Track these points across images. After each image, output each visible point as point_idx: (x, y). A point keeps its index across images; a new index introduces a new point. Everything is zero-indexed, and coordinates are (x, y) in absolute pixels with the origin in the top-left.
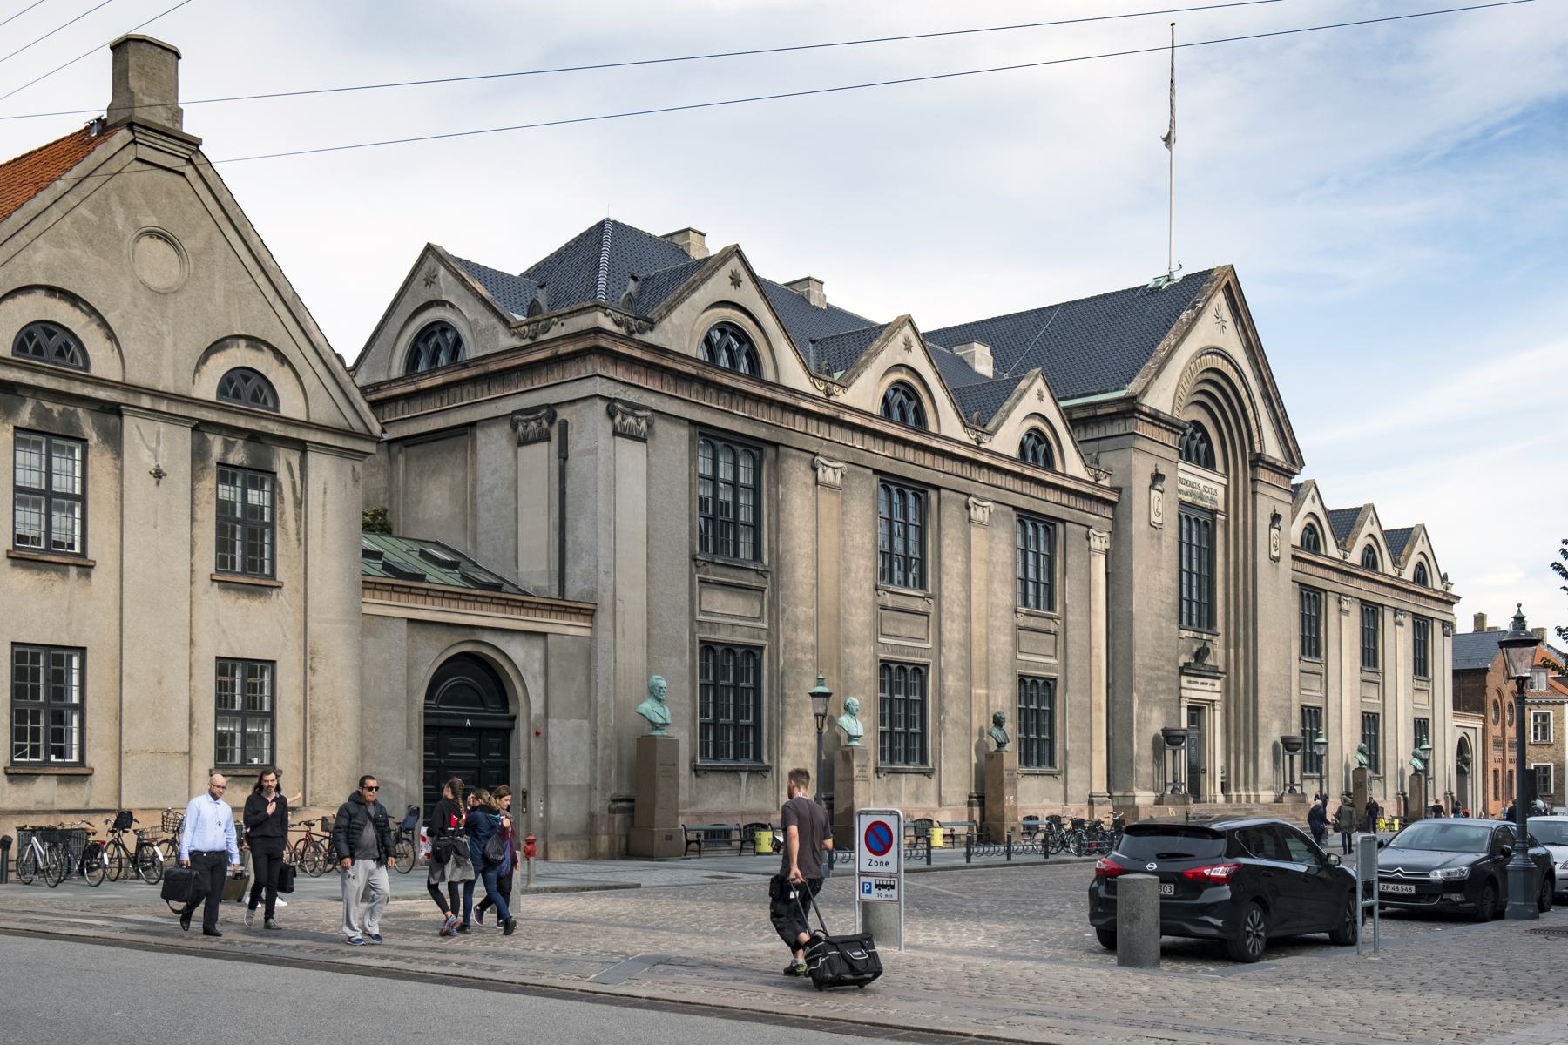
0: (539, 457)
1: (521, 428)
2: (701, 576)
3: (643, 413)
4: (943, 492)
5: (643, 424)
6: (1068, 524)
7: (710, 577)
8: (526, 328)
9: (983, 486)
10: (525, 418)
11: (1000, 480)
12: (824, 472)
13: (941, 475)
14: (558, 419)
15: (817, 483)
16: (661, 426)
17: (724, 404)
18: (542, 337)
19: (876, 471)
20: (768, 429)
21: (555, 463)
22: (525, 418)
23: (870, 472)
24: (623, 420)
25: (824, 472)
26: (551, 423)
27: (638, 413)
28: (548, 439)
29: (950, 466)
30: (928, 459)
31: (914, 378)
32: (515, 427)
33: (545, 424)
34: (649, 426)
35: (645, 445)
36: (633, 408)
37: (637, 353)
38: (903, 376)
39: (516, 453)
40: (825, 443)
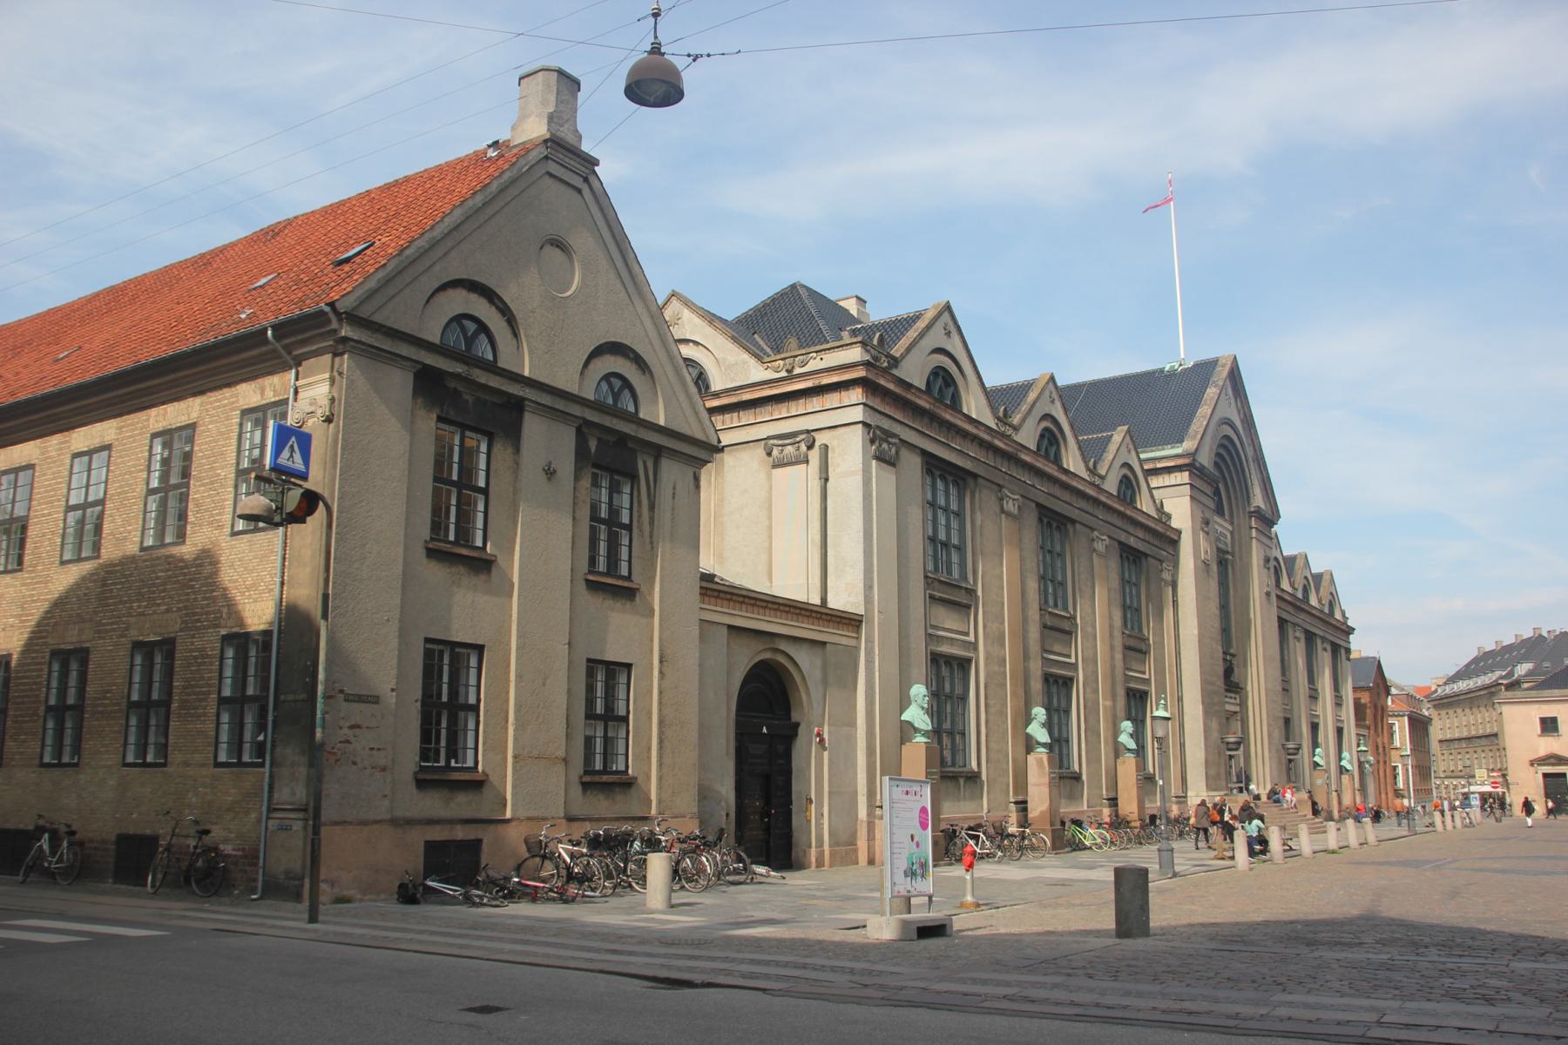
0: (798, 481)
1: (775, 452)
2: (931, 592)
3: (893, 440)
4: (1078, 526)
5: (893, 450)
6: (1149, 559)
7: (938, 594)
8: (781, 362)
9: (1101, 522)
10: (780, 442)
11: (1111, 518)
12: (1007, 502)
13: (1077, 511)
14: (817, 444)
15: (1002, 511)
16: (905, 454)
17: (944, 438)
18: (798, 371)
19: (1038, 505)
20: (971, 461)
21: (815, 485)
22: (780, 442)
23: (1034, 505)
24: (880, 445)
25: (1007, 502)
26: (810, 447)
27: (890, 439)
28: (807, 462)
29: (1082, 504)
30: (1066, 496)
31: (1055, 427)
32: (769, 454)
33: (803, 447)
34: (897, 453)
35: (894, 469)
36: (888, 434)
37: (891, 386)
38: (1052, 426)
39: (769, 477)
40: (1007, 477)
